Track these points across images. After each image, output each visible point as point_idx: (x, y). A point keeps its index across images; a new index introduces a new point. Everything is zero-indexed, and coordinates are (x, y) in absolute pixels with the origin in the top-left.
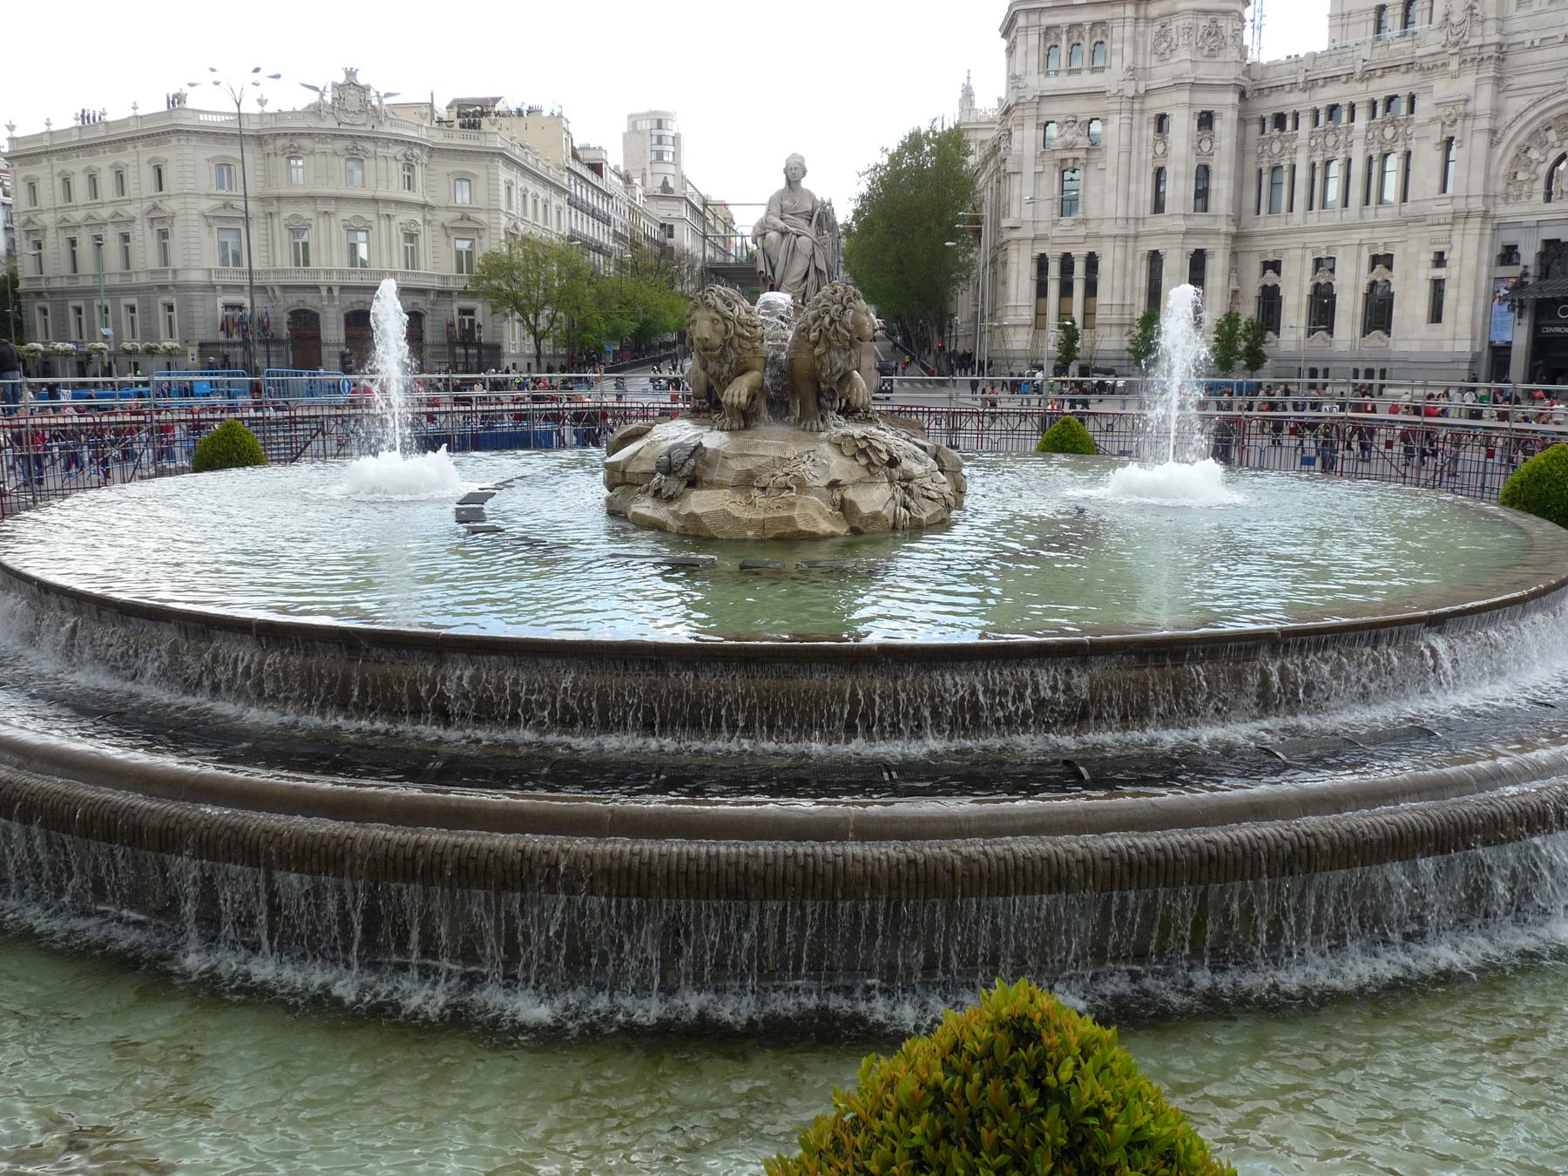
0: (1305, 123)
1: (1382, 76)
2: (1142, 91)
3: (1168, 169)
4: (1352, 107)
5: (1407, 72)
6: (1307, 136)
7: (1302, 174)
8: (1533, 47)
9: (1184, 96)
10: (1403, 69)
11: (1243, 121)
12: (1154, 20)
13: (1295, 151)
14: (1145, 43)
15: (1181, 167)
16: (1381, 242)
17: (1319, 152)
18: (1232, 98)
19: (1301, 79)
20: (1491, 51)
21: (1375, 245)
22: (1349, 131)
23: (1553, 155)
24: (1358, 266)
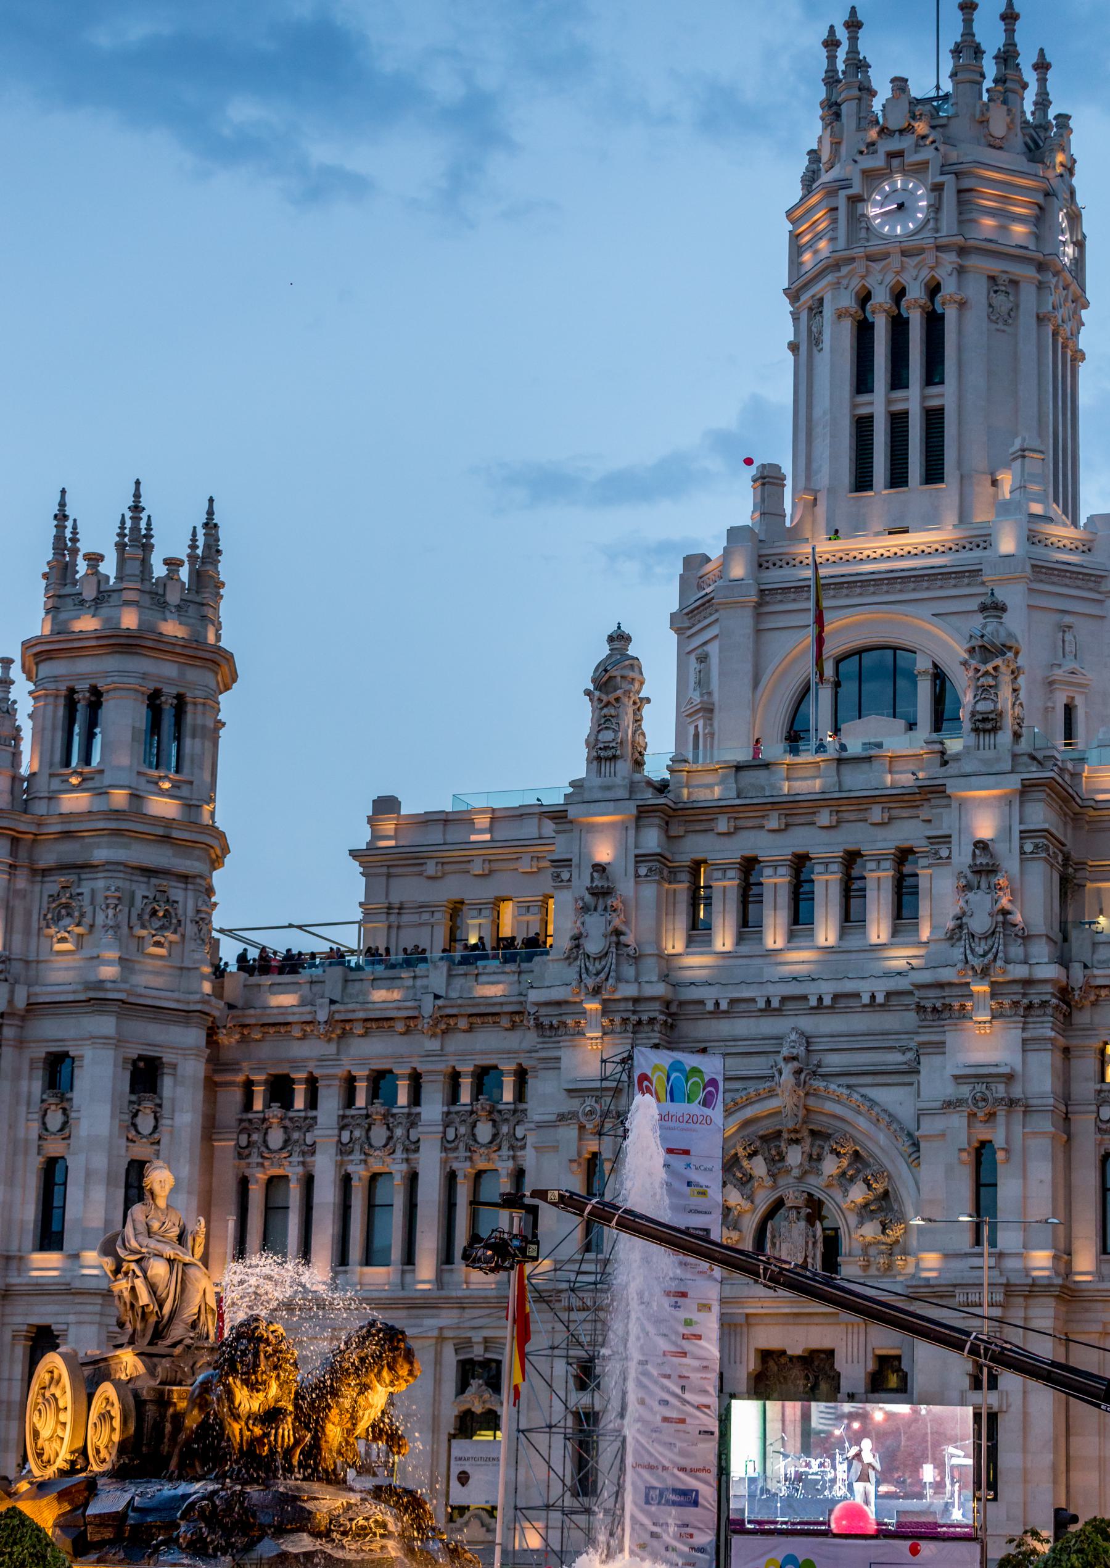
0: (330, 1104)
1: (470, 1029)
2: (21, 1003)
3: (71, 1162)
4: (416, 1079)
5: (513, 1027)
6: (333, 1121)
7: (326, 1194)
8: (717, 1012)
9: (106, 1025)
10: (505, 1022)
11: (211, 1086)
12: (45, 872)
13: (312, 1150)
14: (28, 913)
15: (100, 1161)
16: (477, 1337)
17: (357, 1156)
18: (195, 1036)
19: (322, 1016)
20: (653, 1010)
21: (468, 1343)
22: (413, 1121)
23: (764, 1199)
24: (438, 1382)
